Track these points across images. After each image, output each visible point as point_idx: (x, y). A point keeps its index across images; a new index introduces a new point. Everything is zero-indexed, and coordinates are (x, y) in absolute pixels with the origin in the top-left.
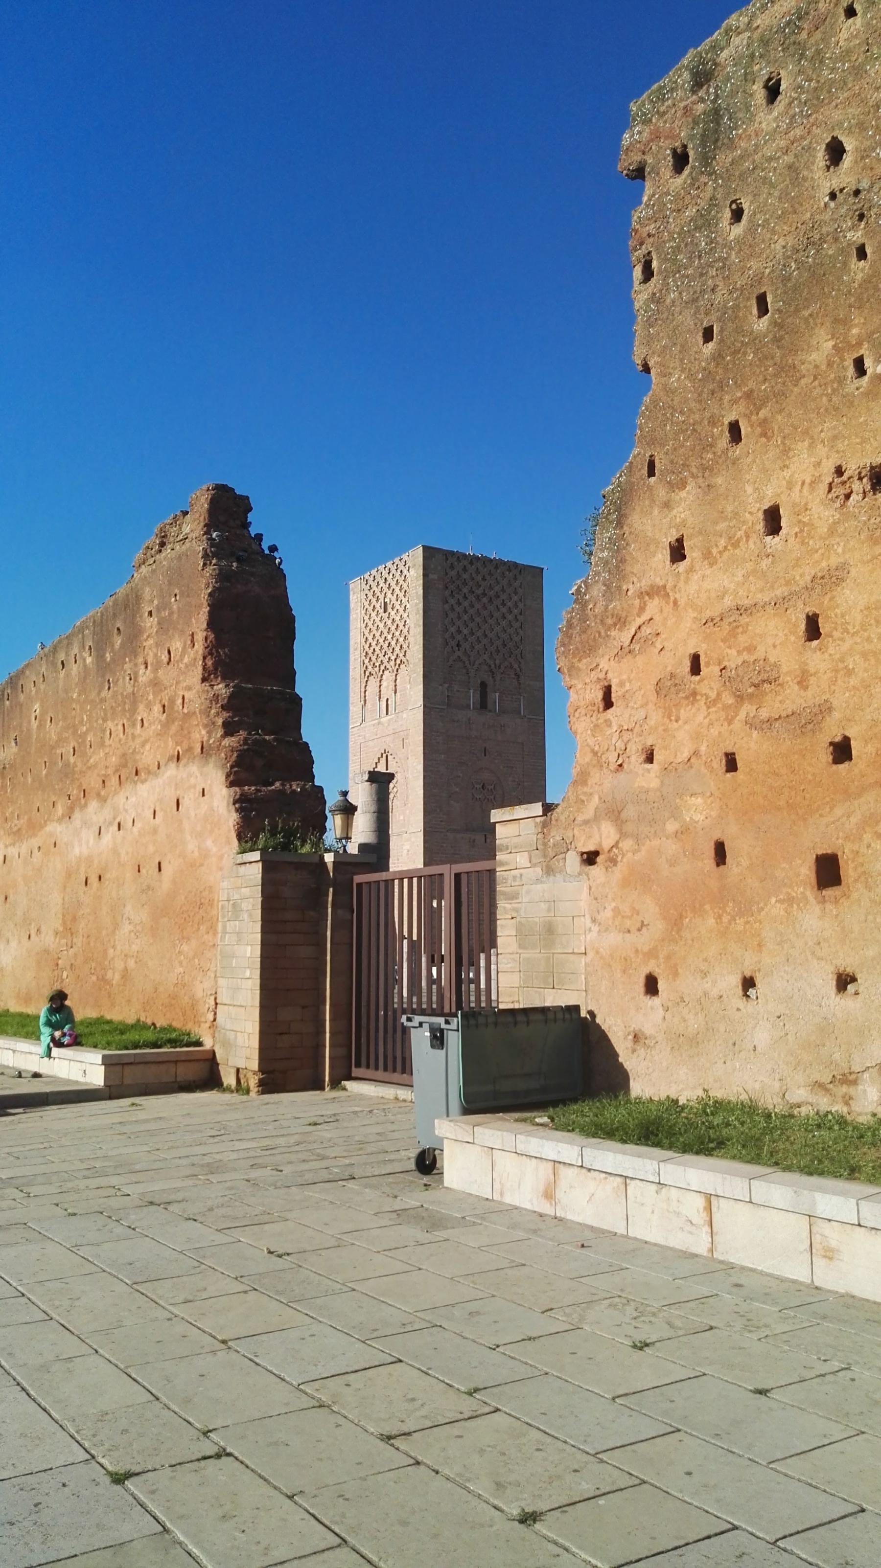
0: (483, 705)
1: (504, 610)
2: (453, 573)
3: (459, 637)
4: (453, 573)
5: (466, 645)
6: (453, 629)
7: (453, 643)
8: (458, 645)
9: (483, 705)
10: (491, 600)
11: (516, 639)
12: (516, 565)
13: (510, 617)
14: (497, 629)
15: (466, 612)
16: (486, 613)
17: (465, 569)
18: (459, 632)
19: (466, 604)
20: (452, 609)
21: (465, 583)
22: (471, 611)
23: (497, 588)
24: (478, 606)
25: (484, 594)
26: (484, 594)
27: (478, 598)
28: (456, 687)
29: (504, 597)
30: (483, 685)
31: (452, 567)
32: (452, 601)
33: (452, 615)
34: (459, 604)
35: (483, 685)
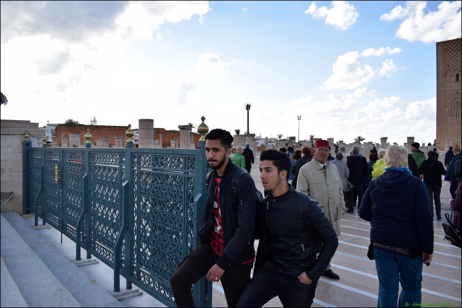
2: (446, 47)
3: (448, 64)
5: (450, 65)
7: (446, 66)
15: (450, 56)
17: (450, 44)
18: (448, 62)
19: (451, 54)
20: (446, 56)
22: (453, 55)
24: (455, 53)
25: (457, 49)
26: (457, 49)
28: (448, 77)
31: (446, 45)
32: (446, 54)
33: (446, 58)
34: (448, 54)
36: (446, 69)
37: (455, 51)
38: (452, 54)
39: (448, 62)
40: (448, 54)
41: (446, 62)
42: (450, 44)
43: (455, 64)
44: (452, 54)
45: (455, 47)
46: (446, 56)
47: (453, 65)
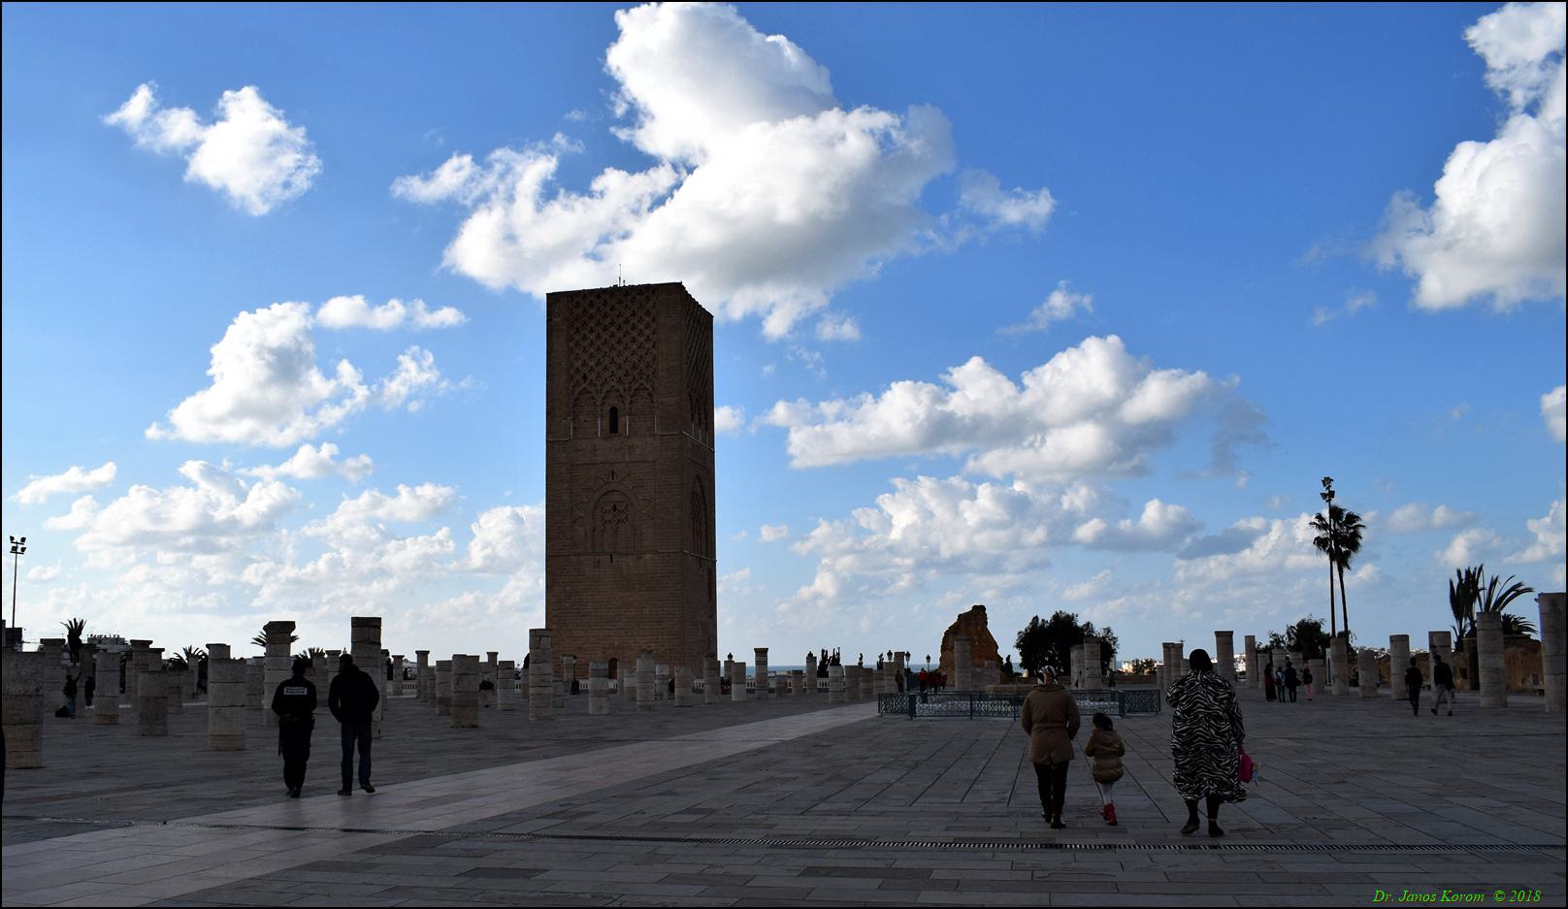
0: (614, 428)
1: (634, 334)
2: (580, 311)
3: (585, 370)
4: (580, 311)
5: (592, 376)
6: (578, 364)
7: (579, 377)
8: (585, 377)
9: (614, 428)
10: (619, 328)
11: (649, 358)
12: (648, 287)
13: (641, 339)
14: (627, 353)
15: (592, 343)
16: (613, 341)
17: (591, 305)
18: (585, 364)
19: (592, 337)
20: (577, 344)
21: (591, 317)
23: (628, 314)
24: (605, 336)
25: (612, 323)
26: (612, 323)
27: (605, 329)
28: (582, 418)
29: (634, 321)
30: (614, 411)
31: (578, 305)
32: (577, 337)
34: (585, 338)
35: (614, 411)
36: (578, 390)
37: (605, 329)
38: (598, 336)
39: (585, 364)
40: (585, 338)
41: (578, 364)
42: (591, 305)
43: (607, 374)
44: (598, 336)
45: (606, 316)
46: (577, 344)
47: (598, 376)
